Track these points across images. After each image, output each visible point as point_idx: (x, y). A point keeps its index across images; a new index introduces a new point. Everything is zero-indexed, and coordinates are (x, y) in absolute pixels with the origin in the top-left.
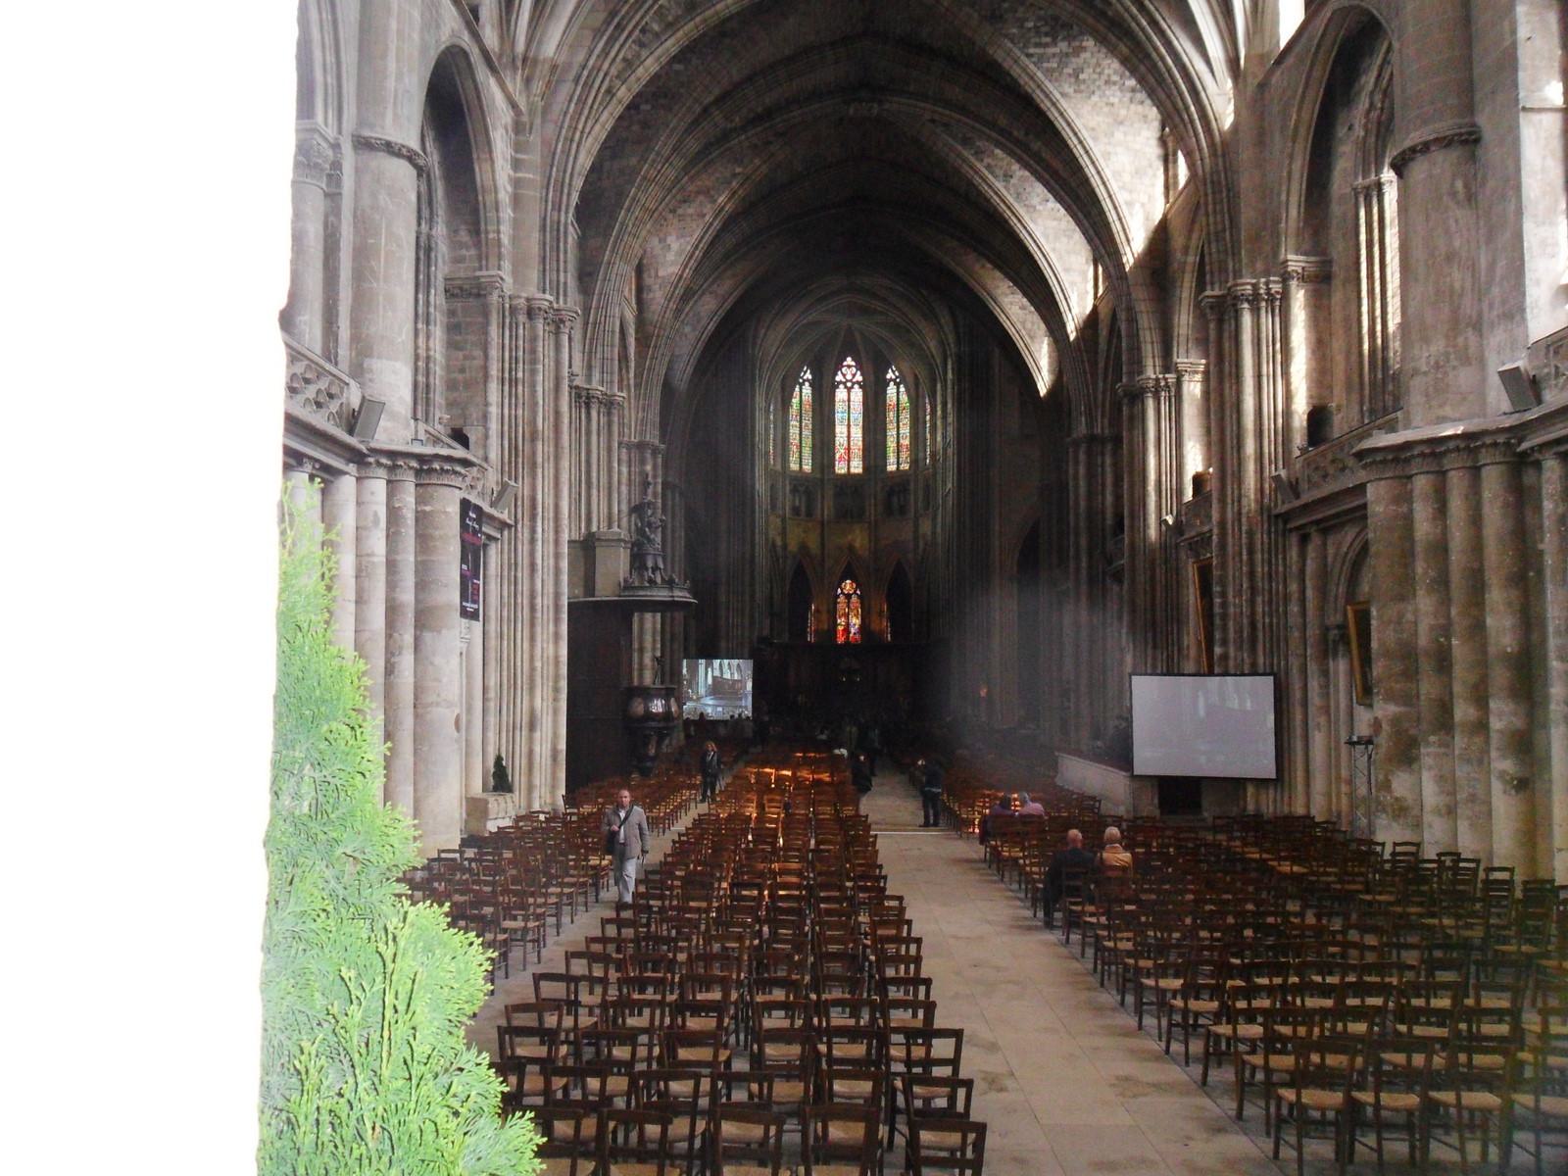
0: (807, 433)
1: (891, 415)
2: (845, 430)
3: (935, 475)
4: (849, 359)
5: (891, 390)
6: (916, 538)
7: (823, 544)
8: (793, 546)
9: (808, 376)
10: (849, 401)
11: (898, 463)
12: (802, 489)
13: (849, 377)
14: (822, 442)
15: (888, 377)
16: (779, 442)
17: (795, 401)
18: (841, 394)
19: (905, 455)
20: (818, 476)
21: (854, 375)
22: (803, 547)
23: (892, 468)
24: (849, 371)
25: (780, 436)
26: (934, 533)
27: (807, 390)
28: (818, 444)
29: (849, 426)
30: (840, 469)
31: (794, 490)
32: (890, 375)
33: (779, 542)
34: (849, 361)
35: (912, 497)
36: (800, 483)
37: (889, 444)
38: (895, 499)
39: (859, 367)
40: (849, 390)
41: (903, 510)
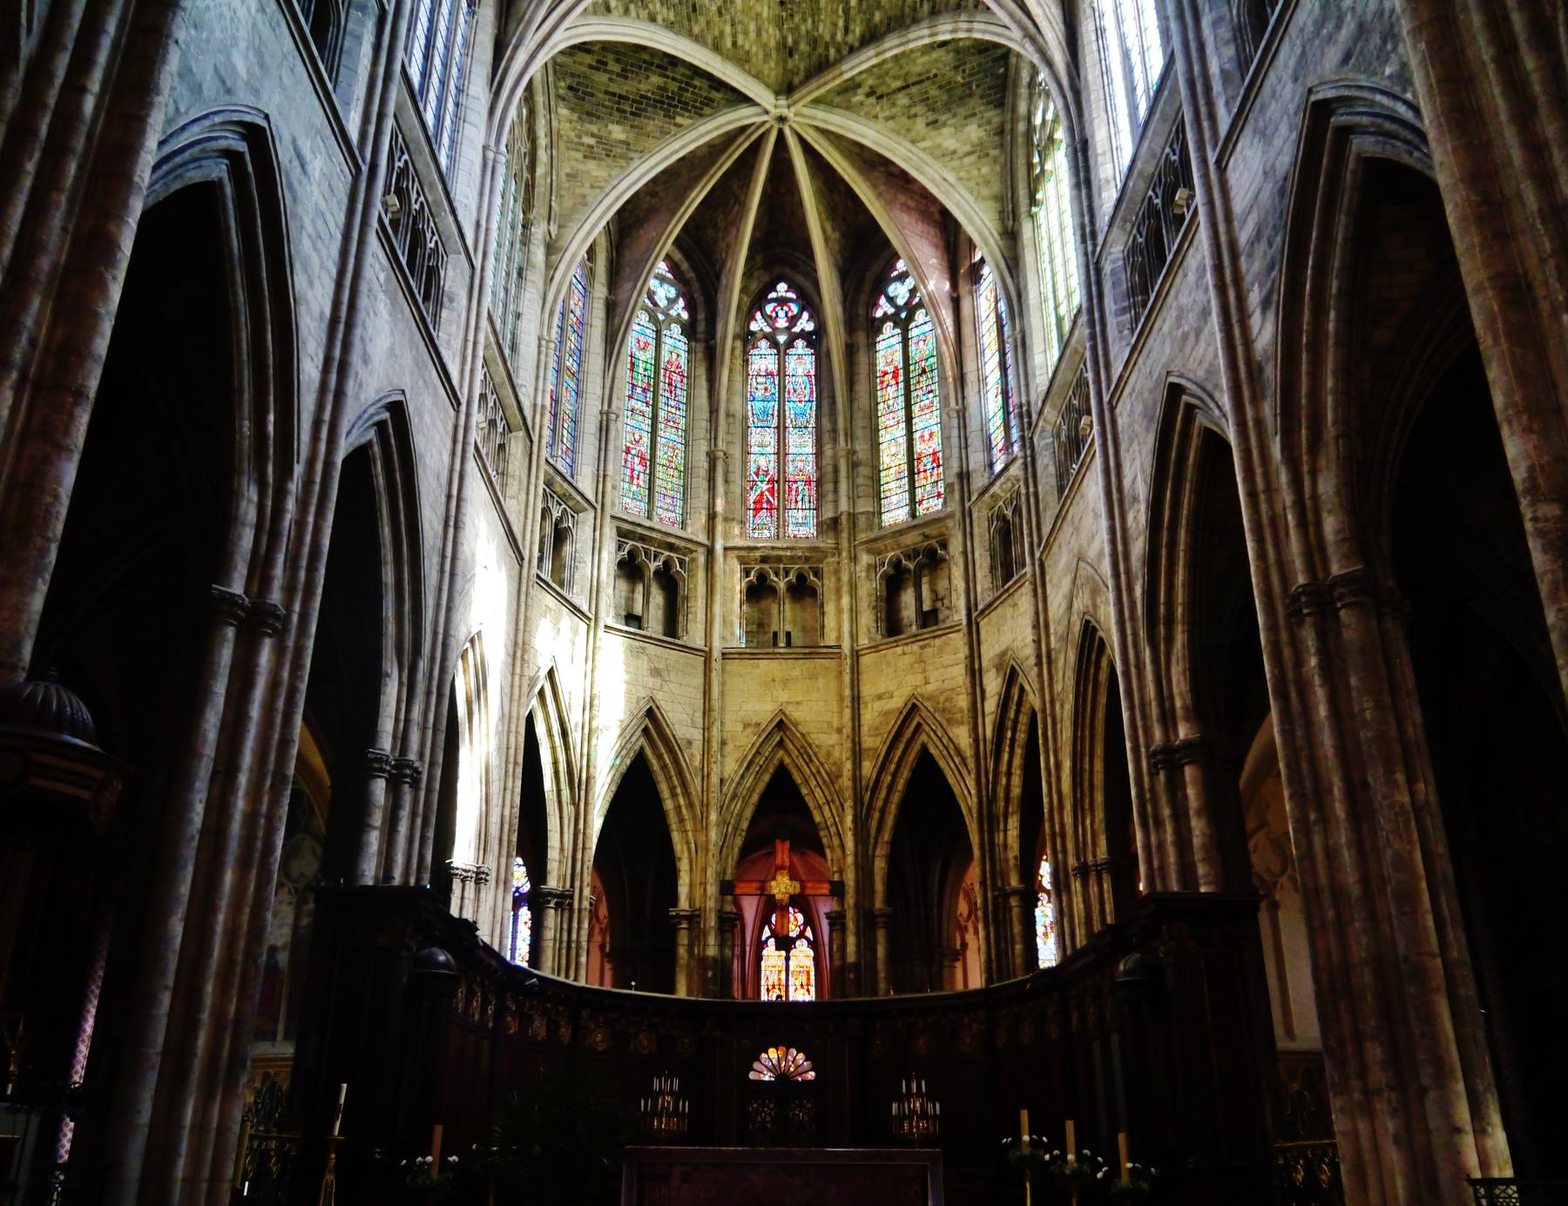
0: (669, 436)
1: (891, 395)
2: (770, 437)
3: (1031, 464)
4: (782, 287)
6: (975, 673)
7: (707, 711)
9: (679, 308)
11: (913, 502)
12: (653, 566)
13: (782, 323)
14: (712, 459)
15: (879, 314)
16: (590, 426)
18: (763, 360)
20: (702, 538)
21: (793, 320)
23: (895, 513)
26: (1040, 625)
27: (676, 345)
28: (702, 463)
29: (781, 429)
30: (762, 533)
31: (630, 569)
32: (884, 308)
35: (957, 573)
37: (885, 460)
38: (908, 598)
39: (809, 301)
40: (782, 351)
41: (928, 619)
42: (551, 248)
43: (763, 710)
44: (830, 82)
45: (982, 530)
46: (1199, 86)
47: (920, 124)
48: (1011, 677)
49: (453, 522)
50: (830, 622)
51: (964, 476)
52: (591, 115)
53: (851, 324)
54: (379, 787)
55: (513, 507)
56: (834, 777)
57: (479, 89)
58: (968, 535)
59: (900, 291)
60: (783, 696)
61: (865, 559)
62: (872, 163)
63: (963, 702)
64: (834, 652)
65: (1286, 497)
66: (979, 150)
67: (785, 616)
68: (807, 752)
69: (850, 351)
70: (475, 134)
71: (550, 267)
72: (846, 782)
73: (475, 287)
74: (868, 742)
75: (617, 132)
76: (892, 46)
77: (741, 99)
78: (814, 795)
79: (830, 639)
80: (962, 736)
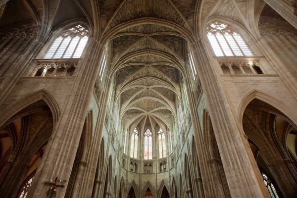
1: (160, 143)
2: (147, 147)
5: (160, 136)
6: (170, 177)
8: (130, 181)
9: (137, 132)
10: (148, 140)
14: (140, 150)
17: (133, 137)
18: (146, 138)
19: (165, 153)
22: (134, 182)
24: (148, 132)
25: (128, 145)
26: (176, 172)
27: (136, 136)
30: (146, 158)
31: (131, 163)
32: (159, 132)
33: (125, 178)
34: (148, 130)
36: (134, 163)
38: (162, 167)
39: (151, 131)
40: (148, 137)
41: (165, 169)
42: (123, 129)
43: (146, 181)
44: (153, 111)
45: (170, 159)
46: (186, 126)
47: (162, 115)
48: (174, 178)
49: (115, 165)
50: (154, 169)
51: (168, 153)
52: (128, 114)
53: (156, 134)
54: (107, 196)
55: (119, 159)
56: (154, 189)
57: (118, 118)
58: (169, 160)
59: (161, 130)
60: (148, 179)
61: (157, 162)
62: (157, 118)
63: (168, 180)
64: (154, 174)
65: (193, 170)
66: (168, 118)
67: (148, 168)
68: (151, 186)
69: (156, 137)
70: (117, 123)
71: (123, 131)
72: (156, 190)
73: (117, 139)
74: (158, 185)
75: (131, 116)
76: (159, 108)
77: (143, 112)
78: (152, 191)
79: (154, 172)
80: (169, 184)
